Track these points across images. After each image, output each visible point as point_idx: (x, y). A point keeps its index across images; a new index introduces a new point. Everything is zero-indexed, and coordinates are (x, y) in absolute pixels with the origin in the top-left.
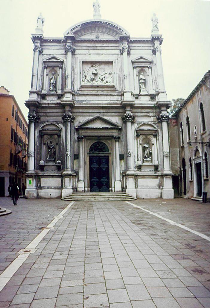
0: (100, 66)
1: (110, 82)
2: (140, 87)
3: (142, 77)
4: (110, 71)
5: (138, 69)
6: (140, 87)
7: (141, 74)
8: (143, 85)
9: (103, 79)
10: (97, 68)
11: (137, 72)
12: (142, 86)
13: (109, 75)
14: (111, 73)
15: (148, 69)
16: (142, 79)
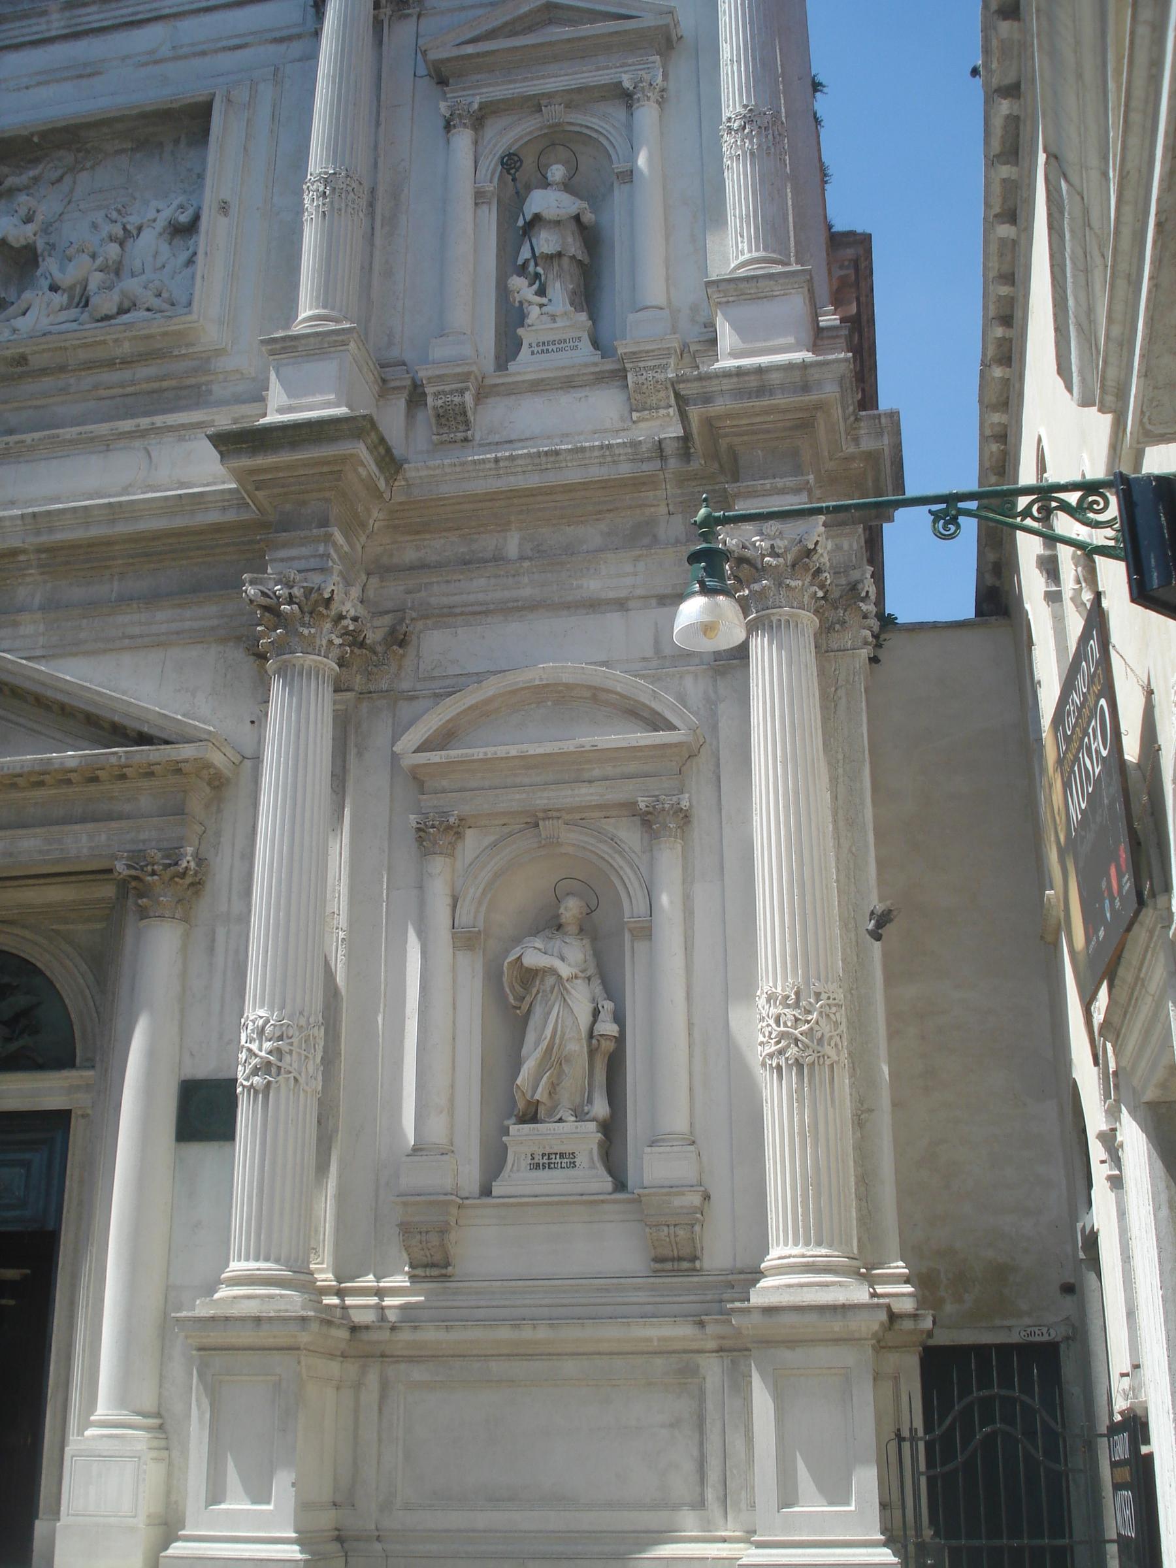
0: (84, 176)
1: (155, 302)
2: (511, 320)
3: (543, 202)
4: (175, 203)
5: (506, 135)
6: (511, 320)
7: (545, 184)
8: (559, 292)
9: (92, 286)
10: (47, 206)
11: (490, 163)
12: (541, 292)
13: (164, 248)
14: (184, 218)
15: (618, 112)
16: (537, 218)
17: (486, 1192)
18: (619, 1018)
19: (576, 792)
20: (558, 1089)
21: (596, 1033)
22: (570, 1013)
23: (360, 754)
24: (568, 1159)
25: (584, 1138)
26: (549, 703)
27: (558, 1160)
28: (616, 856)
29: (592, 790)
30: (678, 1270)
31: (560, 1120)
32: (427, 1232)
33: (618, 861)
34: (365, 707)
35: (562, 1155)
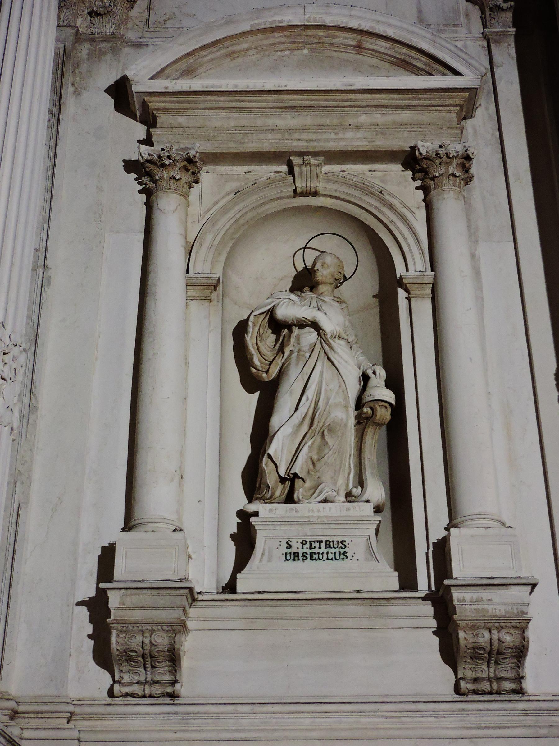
17: (230, 587)
18: (395, 382)
19: (341, 136)
20: (318, 465)
21: (367, 398)
22: (330, 378)
23: (77, 93)
24: (337, 549)
25: (360, 521)
26: (306, 51)
27: (323, 549)
28: (386, 210)
29: (359, 135)
30: (498, 693)
31: (325, 501)
32: (153, 631)
33: (388, 215)
34: (84, 49)
35: (328, 544)
